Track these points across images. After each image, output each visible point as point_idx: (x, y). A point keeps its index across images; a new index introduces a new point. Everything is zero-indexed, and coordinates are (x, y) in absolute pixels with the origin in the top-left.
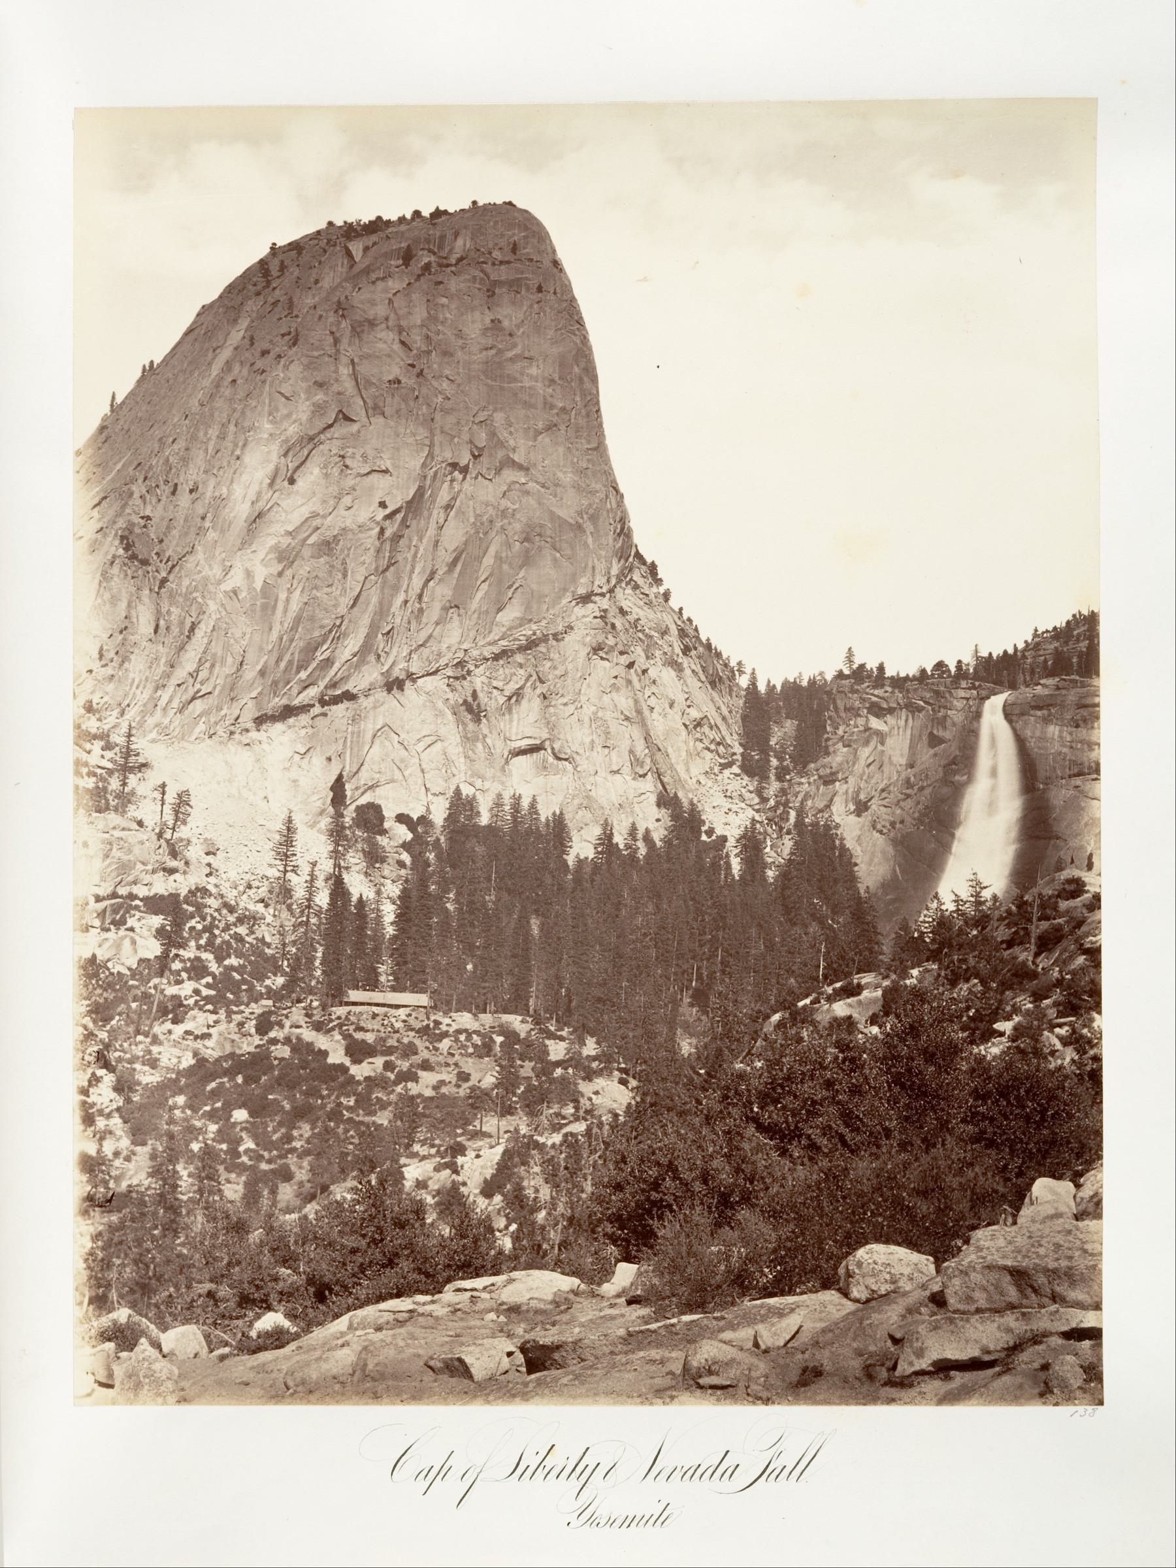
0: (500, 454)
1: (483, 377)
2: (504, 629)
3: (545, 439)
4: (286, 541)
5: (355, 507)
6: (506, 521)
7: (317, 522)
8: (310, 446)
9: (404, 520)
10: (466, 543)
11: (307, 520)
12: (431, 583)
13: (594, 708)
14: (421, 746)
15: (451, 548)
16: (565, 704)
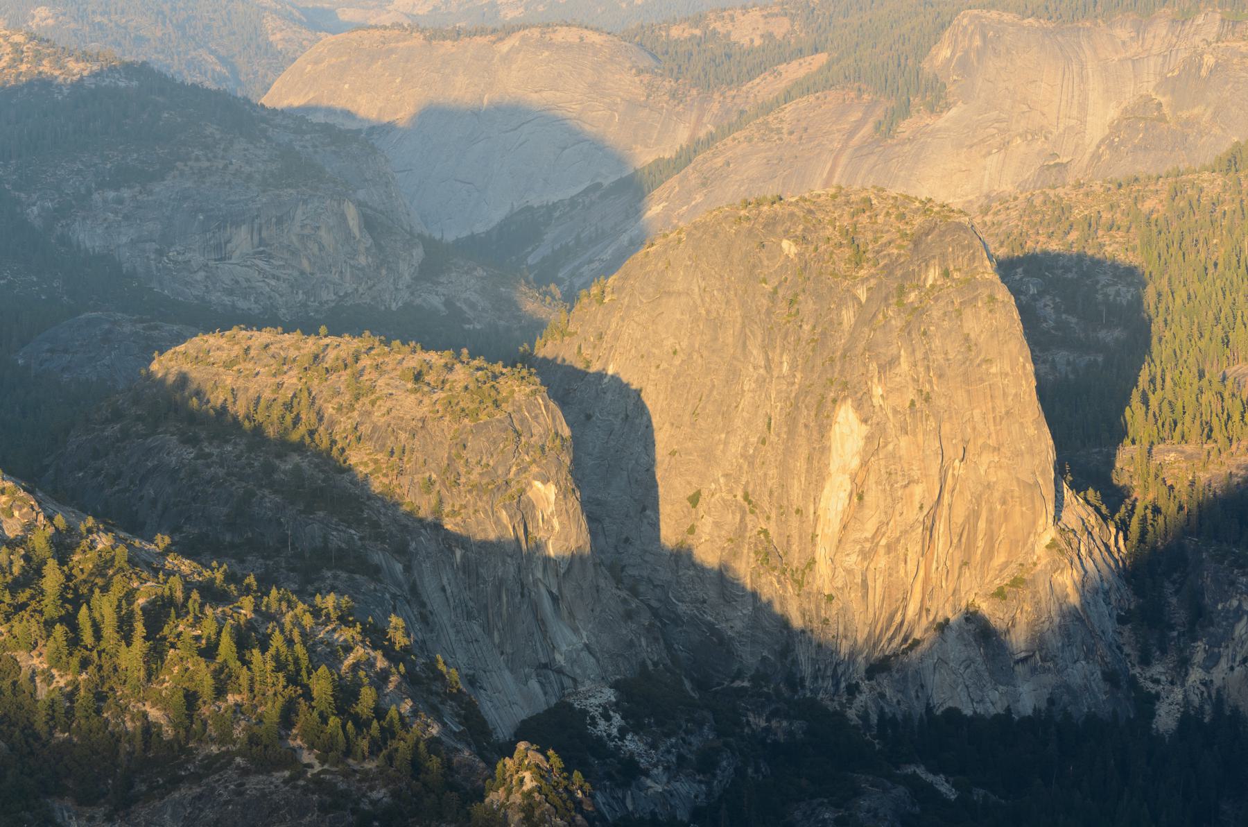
0: (980, 442)
11: (878, 529)
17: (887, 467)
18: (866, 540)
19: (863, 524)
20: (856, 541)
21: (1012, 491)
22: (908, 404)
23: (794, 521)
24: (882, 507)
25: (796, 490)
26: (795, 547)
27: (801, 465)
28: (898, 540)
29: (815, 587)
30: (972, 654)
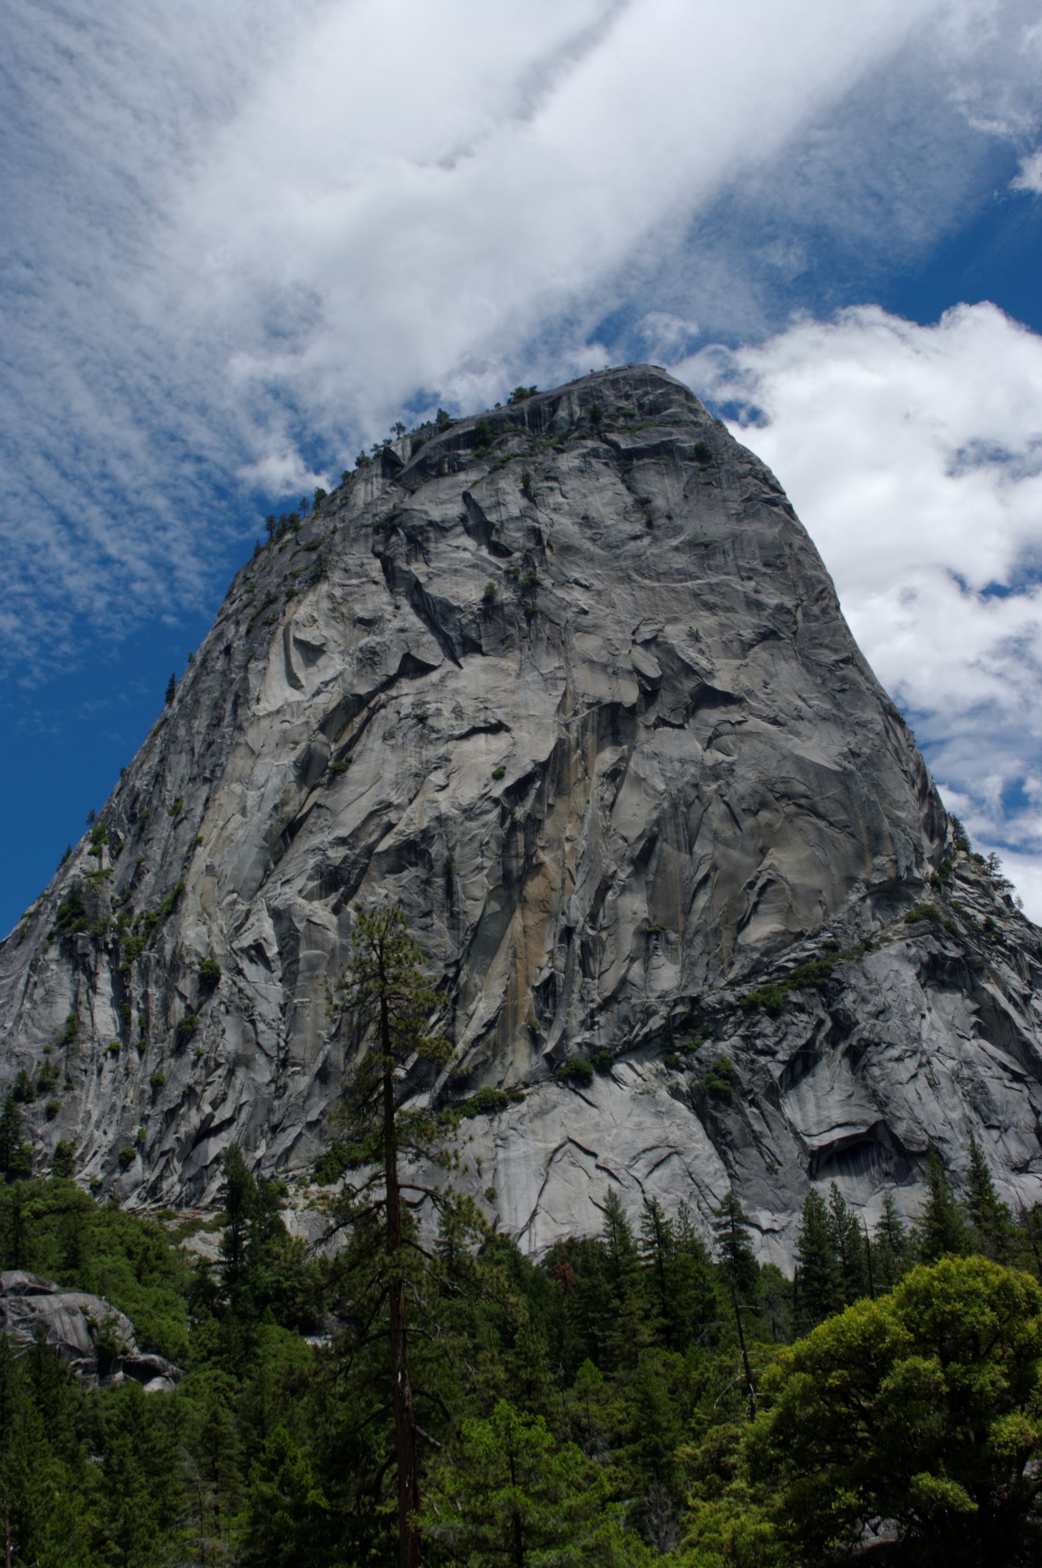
0: (689, 685)
1: (636, 577)
2: (756, 956)
3: (760, 653)
4: (337, 855)
5: (452, 786)
6: (721, 782)
7: (392, 816)
8: (365, 713)
9: (540, 795)
10: (658, 822)
11: (372, 815)
12: (610, 896)
13: (950, 1064)
14: (640, 1169)
15: (633, 834)
16: (899, 1059)
17: (415, 705)
18: (342, 841)
19: (334, 813)
20: (314, 850)
21: (785, 781)
22: (482, 595)
23: (162, 829)
24: (389, 776)
25: (181, 766)
26: (149, 878)
27: (200, 724)
28: (426, 835)
29: (168, 948)
30: (675, 1135)
